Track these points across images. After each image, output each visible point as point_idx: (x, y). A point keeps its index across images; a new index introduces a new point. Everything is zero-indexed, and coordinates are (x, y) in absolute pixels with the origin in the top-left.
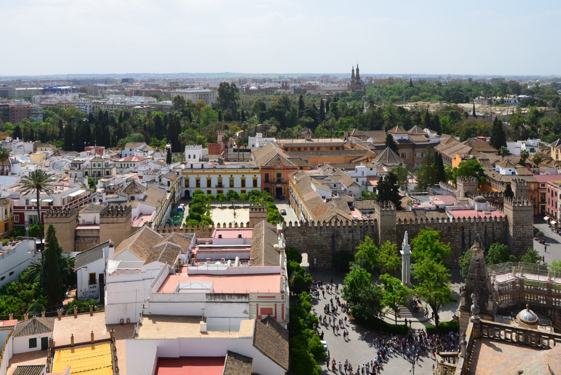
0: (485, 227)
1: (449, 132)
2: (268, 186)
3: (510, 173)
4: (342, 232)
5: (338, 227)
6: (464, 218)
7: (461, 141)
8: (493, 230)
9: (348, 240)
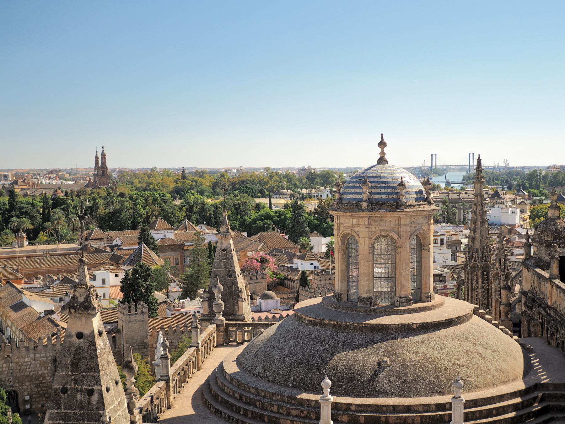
3: (312, 268)
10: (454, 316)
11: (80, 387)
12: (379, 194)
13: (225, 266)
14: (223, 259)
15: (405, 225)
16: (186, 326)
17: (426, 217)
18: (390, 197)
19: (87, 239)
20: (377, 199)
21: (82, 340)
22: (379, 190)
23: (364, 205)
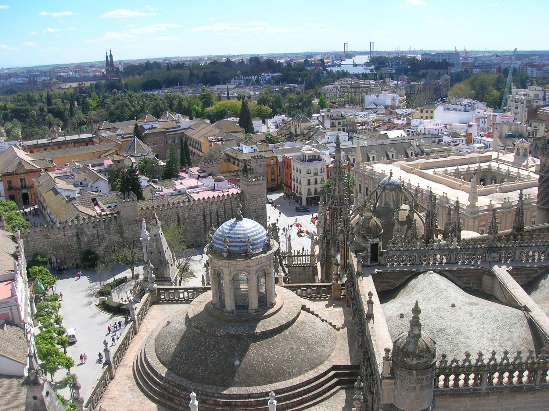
0: (224, 205)
1: (200, 116)
2: (13, 192)
4: (86, 229)
5: (82, 224)
6: (204, 198)
7: (212, 122)
8: (231, 206)
9: (93, 236)
10: (285, 322)
12: (235, 246)
16: (163, 206)
18: (242, 248)
19: (99, 130)
22: (235, 244)
23: (225, 255)
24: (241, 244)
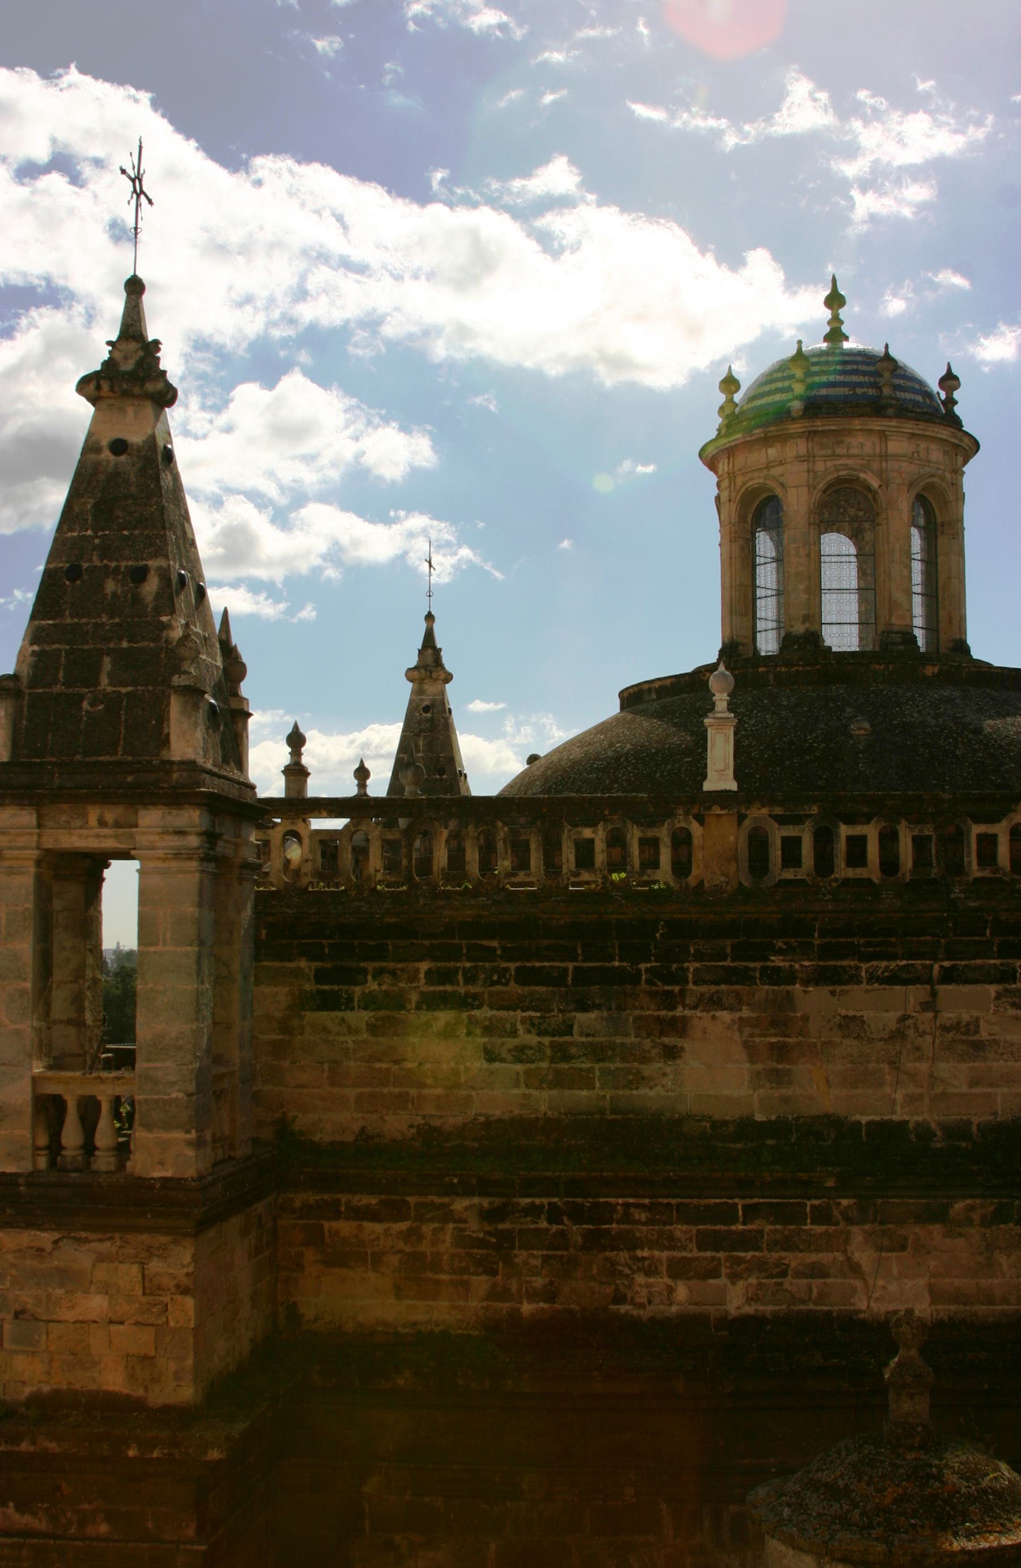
11: (114, 564)
13: (429, 747)
14: (421, 731)
15: (897, 457)
17: (946, 453)
18: (859, 391)
20: (827, 396)
21: (123, 458)
24: (855, 379)
